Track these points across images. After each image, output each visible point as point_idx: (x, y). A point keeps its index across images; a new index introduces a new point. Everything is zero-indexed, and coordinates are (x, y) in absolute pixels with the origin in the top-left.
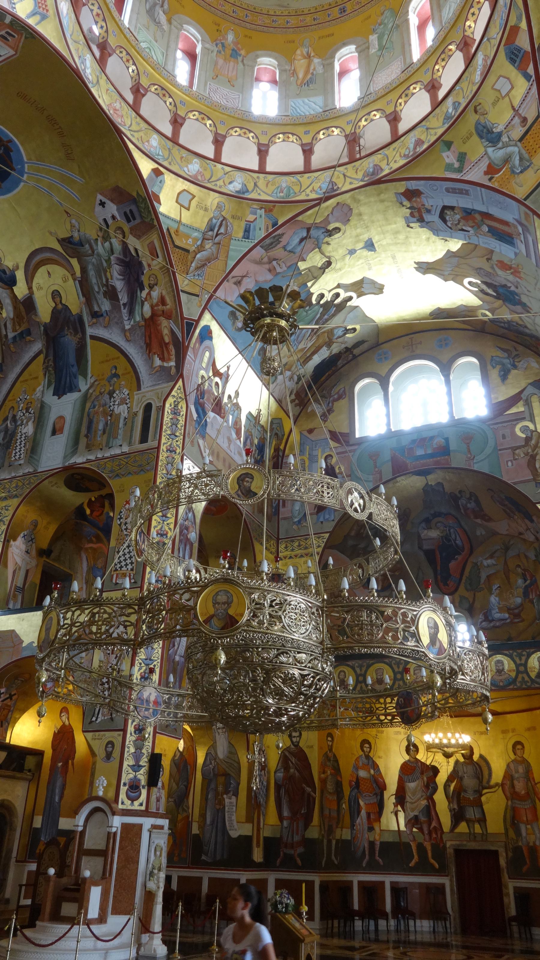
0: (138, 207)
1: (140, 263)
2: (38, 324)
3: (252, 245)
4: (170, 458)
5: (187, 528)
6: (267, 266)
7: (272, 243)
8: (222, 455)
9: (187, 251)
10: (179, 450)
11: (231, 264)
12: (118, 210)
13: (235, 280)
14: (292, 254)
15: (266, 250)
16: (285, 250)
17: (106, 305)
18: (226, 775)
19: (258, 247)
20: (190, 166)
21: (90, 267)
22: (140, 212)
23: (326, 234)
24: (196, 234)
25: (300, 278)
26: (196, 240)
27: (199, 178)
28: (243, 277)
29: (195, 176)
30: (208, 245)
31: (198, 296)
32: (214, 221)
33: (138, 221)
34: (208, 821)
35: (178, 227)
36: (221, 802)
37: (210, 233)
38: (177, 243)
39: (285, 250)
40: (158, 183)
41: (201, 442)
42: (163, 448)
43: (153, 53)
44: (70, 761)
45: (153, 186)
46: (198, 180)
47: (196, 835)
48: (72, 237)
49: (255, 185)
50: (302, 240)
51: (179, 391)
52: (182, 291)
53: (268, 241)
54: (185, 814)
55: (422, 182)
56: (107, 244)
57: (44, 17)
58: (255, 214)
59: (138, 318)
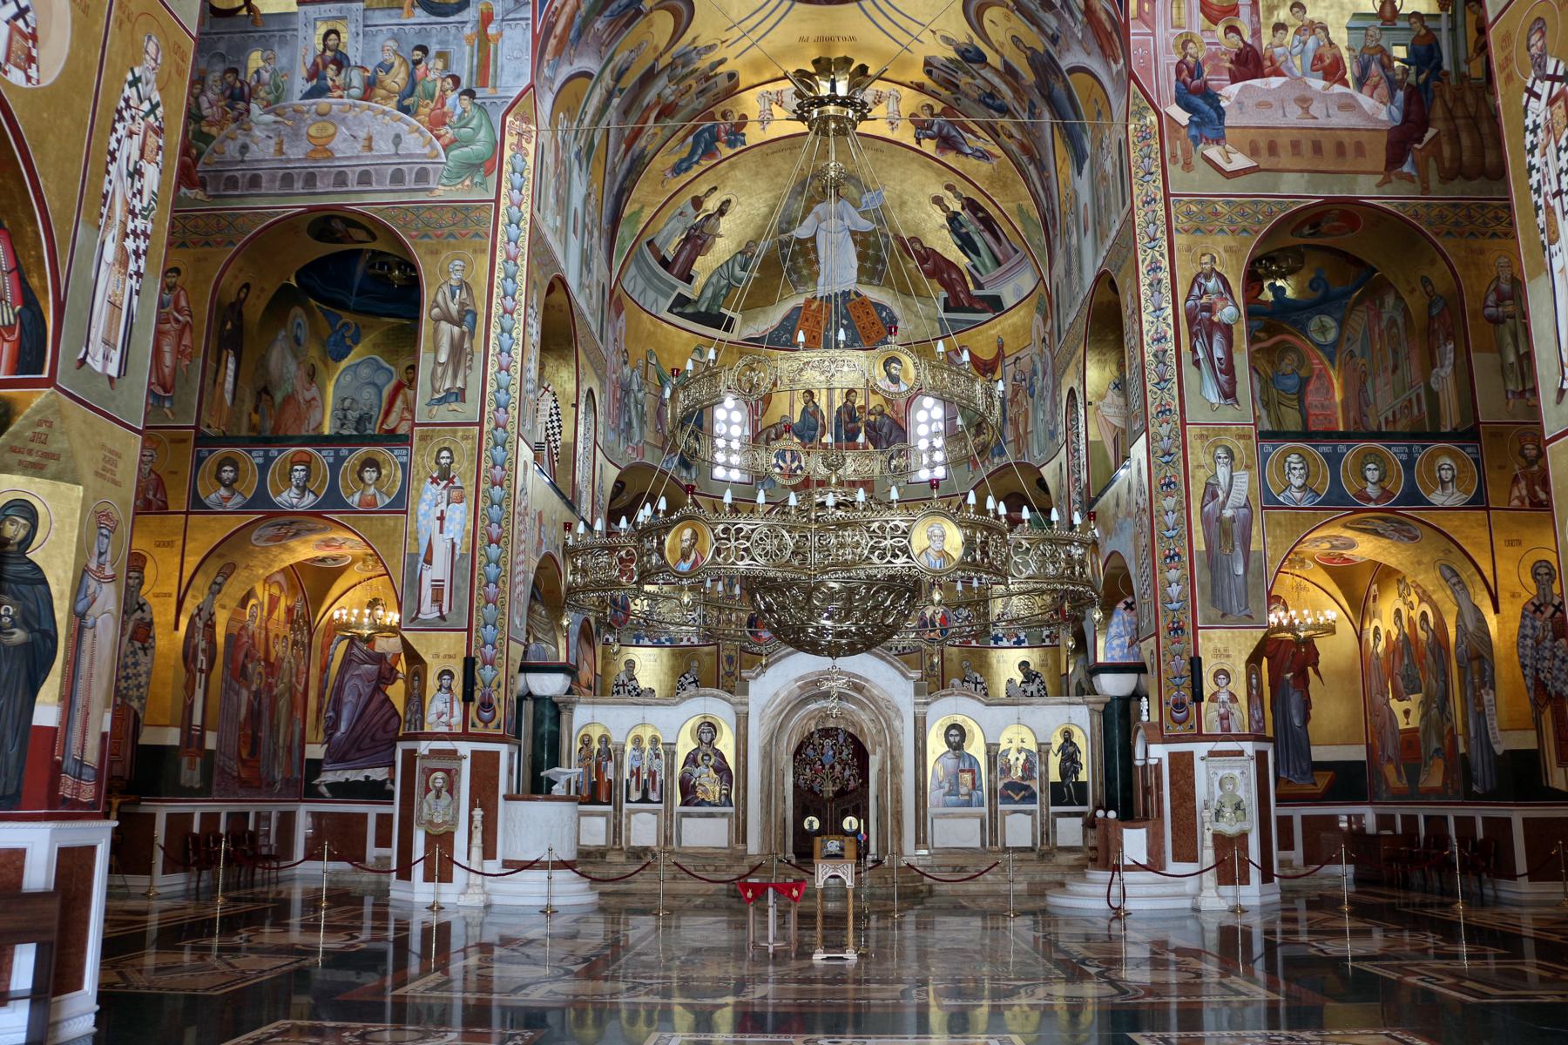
2: (1030, 86)
4: (1150, 214)
5: (1209, 308)
8: (1284, 141)
10: (1160, 195)
17: (1051, 21)
18: (1480, 657)
34: (1472, 735)
36: (1480, 702)
41: (1213, 152)
42: (1138, 203)
44: (1310, 669)
47: (1463, 754)
54: (1449, 725)
59: (1080, 16)
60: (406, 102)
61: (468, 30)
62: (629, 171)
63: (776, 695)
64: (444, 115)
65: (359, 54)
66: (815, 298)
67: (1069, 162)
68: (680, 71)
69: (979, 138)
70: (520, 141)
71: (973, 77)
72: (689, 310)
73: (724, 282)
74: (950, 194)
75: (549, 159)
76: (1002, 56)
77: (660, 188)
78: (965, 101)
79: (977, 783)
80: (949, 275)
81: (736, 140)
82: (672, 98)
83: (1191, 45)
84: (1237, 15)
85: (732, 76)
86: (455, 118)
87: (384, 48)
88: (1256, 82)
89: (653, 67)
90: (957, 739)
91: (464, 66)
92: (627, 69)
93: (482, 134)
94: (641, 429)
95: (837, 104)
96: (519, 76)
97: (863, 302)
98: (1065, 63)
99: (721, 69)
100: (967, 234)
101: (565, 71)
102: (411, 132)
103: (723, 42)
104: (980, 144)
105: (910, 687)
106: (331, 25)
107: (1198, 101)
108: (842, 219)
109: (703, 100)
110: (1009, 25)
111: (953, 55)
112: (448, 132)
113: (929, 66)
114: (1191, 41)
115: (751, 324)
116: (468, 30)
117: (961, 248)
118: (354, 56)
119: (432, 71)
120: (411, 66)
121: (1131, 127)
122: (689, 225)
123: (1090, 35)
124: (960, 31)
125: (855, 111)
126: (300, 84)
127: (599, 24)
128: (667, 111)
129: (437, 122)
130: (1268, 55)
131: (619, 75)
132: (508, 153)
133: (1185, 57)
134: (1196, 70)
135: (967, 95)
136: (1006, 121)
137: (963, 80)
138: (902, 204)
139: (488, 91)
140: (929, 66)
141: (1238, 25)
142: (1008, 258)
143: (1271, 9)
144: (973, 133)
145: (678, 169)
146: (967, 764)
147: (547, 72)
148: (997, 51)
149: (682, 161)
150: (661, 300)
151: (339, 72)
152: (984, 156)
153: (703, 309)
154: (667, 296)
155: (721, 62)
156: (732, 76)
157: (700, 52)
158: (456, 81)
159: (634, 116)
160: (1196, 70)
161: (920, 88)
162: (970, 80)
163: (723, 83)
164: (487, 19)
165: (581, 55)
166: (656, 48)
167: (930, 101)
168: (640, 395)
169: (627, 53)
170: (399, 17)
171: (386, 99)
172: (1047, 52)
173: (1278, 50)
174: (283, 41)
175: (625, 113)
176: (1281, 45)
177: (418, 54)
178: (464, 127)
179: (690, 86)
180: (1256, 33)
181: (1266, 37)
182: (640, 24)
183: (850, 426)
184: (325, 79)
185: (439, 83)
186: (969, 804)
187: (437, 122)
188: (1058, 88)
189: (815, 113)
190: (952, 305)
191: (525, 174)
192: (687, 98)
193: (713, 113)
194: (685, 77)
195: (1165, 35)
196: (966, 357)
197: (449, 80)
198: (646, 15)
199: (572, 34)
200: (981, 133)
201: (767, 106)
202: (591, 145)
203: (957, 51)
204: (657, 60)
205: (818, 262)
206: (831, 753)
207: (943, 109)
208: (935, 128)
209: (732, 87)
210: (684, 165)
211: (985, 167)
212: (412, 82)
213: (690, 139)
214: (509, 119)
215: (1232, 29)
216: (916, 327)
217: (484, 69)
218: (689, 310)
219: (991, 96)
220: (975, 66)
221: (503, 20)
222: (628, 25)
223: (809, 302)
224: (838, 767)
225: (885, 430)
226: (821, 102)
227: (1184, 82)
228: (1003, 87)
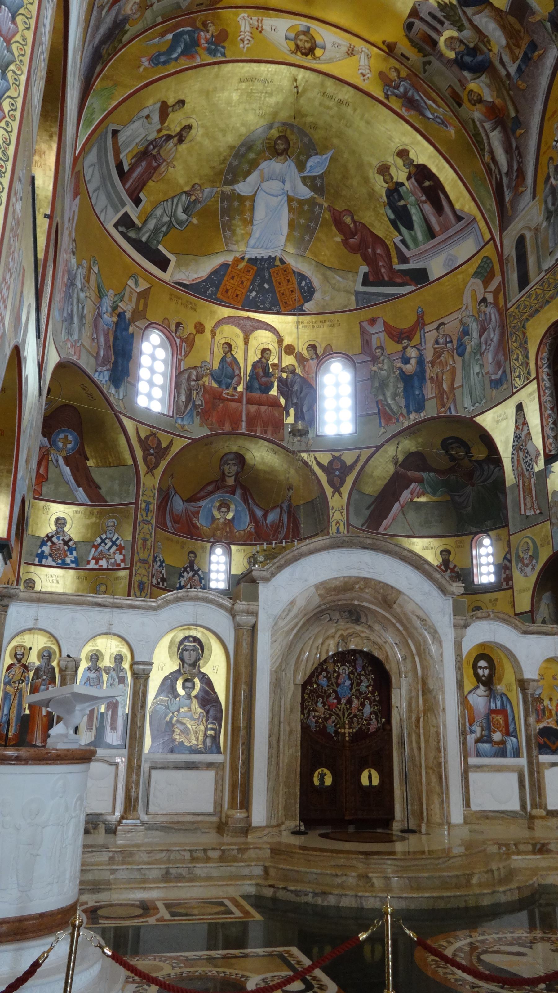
63: (293, 603)
66: (243, 258)
72: (132, 234)
73: (166, 219)
74: (400, 162)
78: (436, 63)
79: (511, 728)
80: (374, 251)
90: (487, 672)
94: (80, 331)
97: (286, 270)
100: (405, 207)
105: (447, 604)
108: (284, 182)
115: (183, 269)
117: (393, 223)
122: (150, 138)
142: (445, 228)
146: (499, 704)
149: (160, 54)
150: (110, 210)
153: (144, 239)
154: (117, 211)
167: (398, 65)
168: (82, 295)
183: (264, 379)
186: (503, 754)
190: (371, 278)
196: (379, 327)
205: (251, 222)
206: (348, 683)
207: (408, 75)
208: (402, 89)
210: (162, 59)
213: (170, 36)
216: (332, 299)
218: (132, 234)
223: (237, 261)
224: (355, 702)
225: (296, 387)
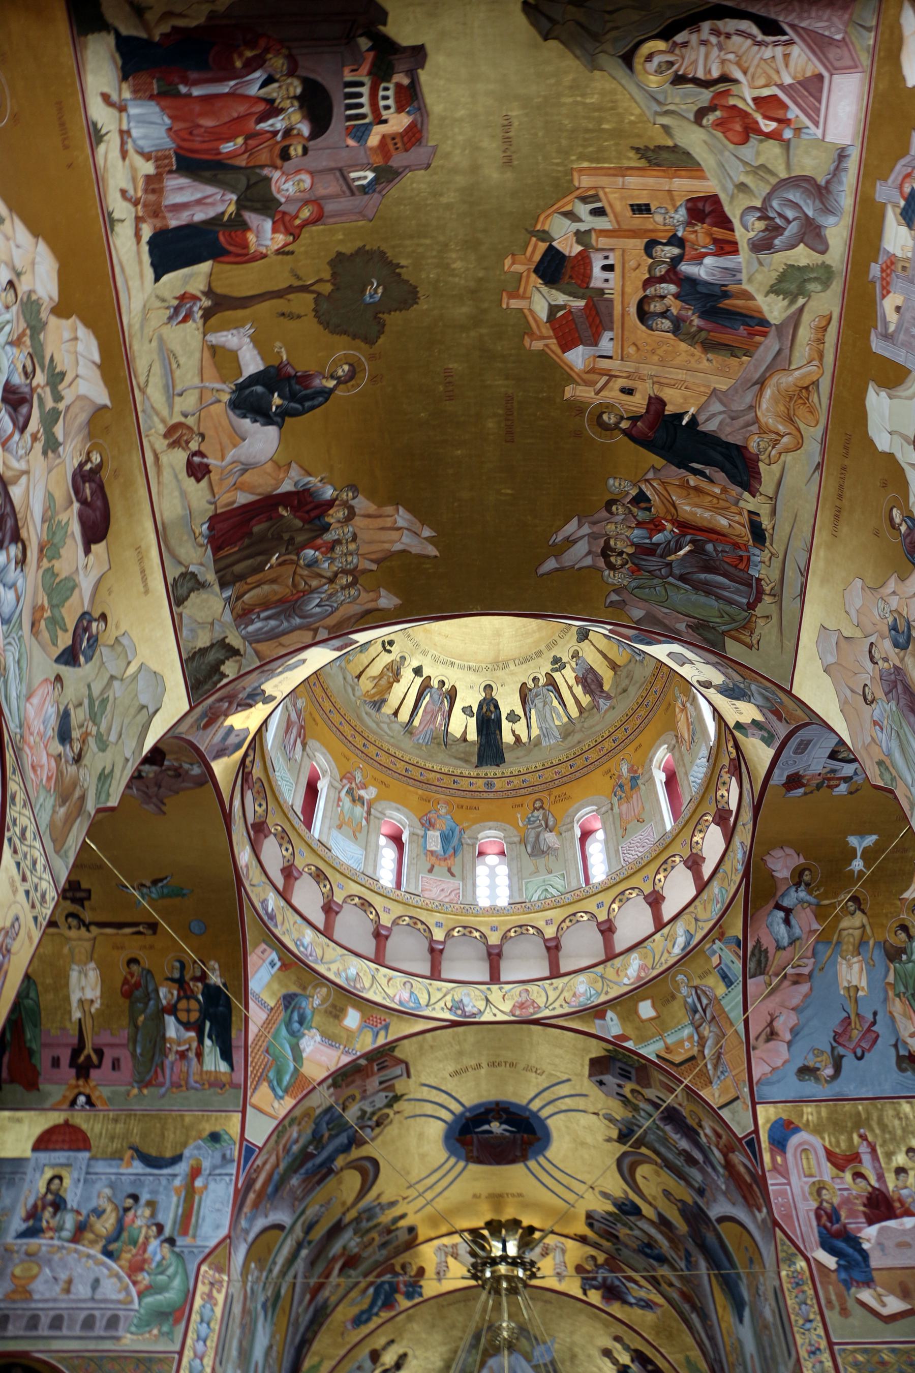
0: (619, 1060)
1: (674, 1108)
3: (741, 986)
6: (786, 983)
7: (759, 962)
9: (693, 1058)
11: (741, 1028)
12: (614, 1076)
13: (763, 1037)
14: (798, 943)
15: (762, 973)
16: (784, 948)
17: (696, 1175)
19: (749, 981)
20: (629, 972)
21: (657, 1145)
22: (625, 1063)
23: (803, 887)
24: (687, 1032)
25: (845, 947)
26: (690, 1037)
27: (643, 974)
28: (770, 1024)
29: (639, 978)
30: (706, 1030)
31: (737, 1098)
32: (690, 1000)
33: (633, 1072)
35: (665, 1043)
37: (697, 1016)
38: (677, 1059)
39: (784, 948)
40: (611, 1023)
43: (551, 890)
45: (609, 1032)
46: (643, 978)
48: (620, 1131)
49: (696, 920)
50: (787, 922)
51: (785, 1248)
52: (720, 1108)
53: (751, 965)
55: (776, 771)
56: (642, 1113)
57: (386, 1028)
58: (715, 952)
59: (721, 1170)
60: (113, 1247)
61: (177, 1182)
62: (312, 1322)
64: (144, 1261)
65: (77, 1199)
67: (729, 1309)
68: (365, 1225)
69: (641, 1286)
70: (211, 1291)
71: (631, 1229)
75: (237, 1309)
76: (655, 1208)
77: (340, 1340)
81: (414, 1292)
82: (356, 1250)
83: (824, 1192)
84: (860, 1162)
85: (412, 1229)
86: (154, 1265)
87: (101, 1194)
88: (891, 1223)
89: (340, 1221)
91: (168, 1217)
92: (317, 1222)
93: (177, 1283)
95: (508, 1263)
96: (218, 1227)
98: (714, 1212)
99: (403, 1223)
101: (261, 1223)
102: (110, 1276)
103: (404, 1199)
104: (642, 1294)
106: (56, 1171)
107: (841, 1245)
109: (384, 1252)
110: (659, 1180)
111: (610, 1208)
112: (144, 1278)
113: (590, 1218)
114: (824, 1188)
116: (177, 1182)
118: (72, 1200)
119: (140, 1218)
120: (121, 1212)
121: (783, 1273)
123: (732, 1187)
124: (616, 1186)
125: (525, 1270)
126: (17, 1224)
127: (295, 1181)
128: (351, 1262)
129: (136, 1268)
130: (896, 1197)
131: (309, 1228)
132: (198, 1302)
133: (821, 1203)
134: (833, 1215)
135: (626, 1246)
136: (664, 1271)
137: (622, 1232)
138: (573, 1357)
139: (188, 1240)
140: (590, 1218)
141: (863, 1171)
143: (889, 1155)
144: (635, 1282)
145: (359, 1321)
147: (243, 1223)
148: (650, 1204)
149: (362, 1312)
151: (55, 1214)
152: (647, 1305)
155: (403, 1216)
156: (412, 1229)
157: (383, 1208)
158: (160, 1228)
159: (320, 1268)
160: (833, 1215)
161: (583, 1239)
162: (629, 1232)
163: (403, 1236)
164: (196, 1172)
165: (275, 1208)
166: (344, 1203)
167: (593, 1252)
169: (317, 1207)
170: (119, 1167)
171: (93, 1243)
172: (696, 1203)
173: (904, 1192)
174: (11, 1183)
175: (312, 1263)
176: (906, 1187)
177: (130, 1202)
178: (162, 1273)
179: (373, 1239)
180: (881, 1177)
181: (891, 1182)
182: (331, 1181)
184: (41, 1220)
185: (144, 1231)
187: (136, 1268)
188: (710, 1237)
189: (488, 1274)
191: (212, 1325)
192: (370, 1250)
193: (393, 1265)
194: (369, 1231)
195: (799, 1185)
197: (154, 1228)
198: (337, 1173)
199: (270, 1189)
200: (643, 1282)
201: (443, 1259)
202: (277, 1296)
203: (615, 1204)
204: (344, 1214)
207: (606, 1260)
209: (412, 1240)
210: (364, 1317)
211: (650, 1317)
212: (120, 1227)
213: (371, 1290)
214: (204, 1268)
215: (858, 1175)
217: (186, 1222)
219: (649, 1246)
220: (632, 1218)
221: (210, 1175)
222: (320, 1182)
226: (494, 1262)
227: (825, 1227)
228: (659, 1237)
